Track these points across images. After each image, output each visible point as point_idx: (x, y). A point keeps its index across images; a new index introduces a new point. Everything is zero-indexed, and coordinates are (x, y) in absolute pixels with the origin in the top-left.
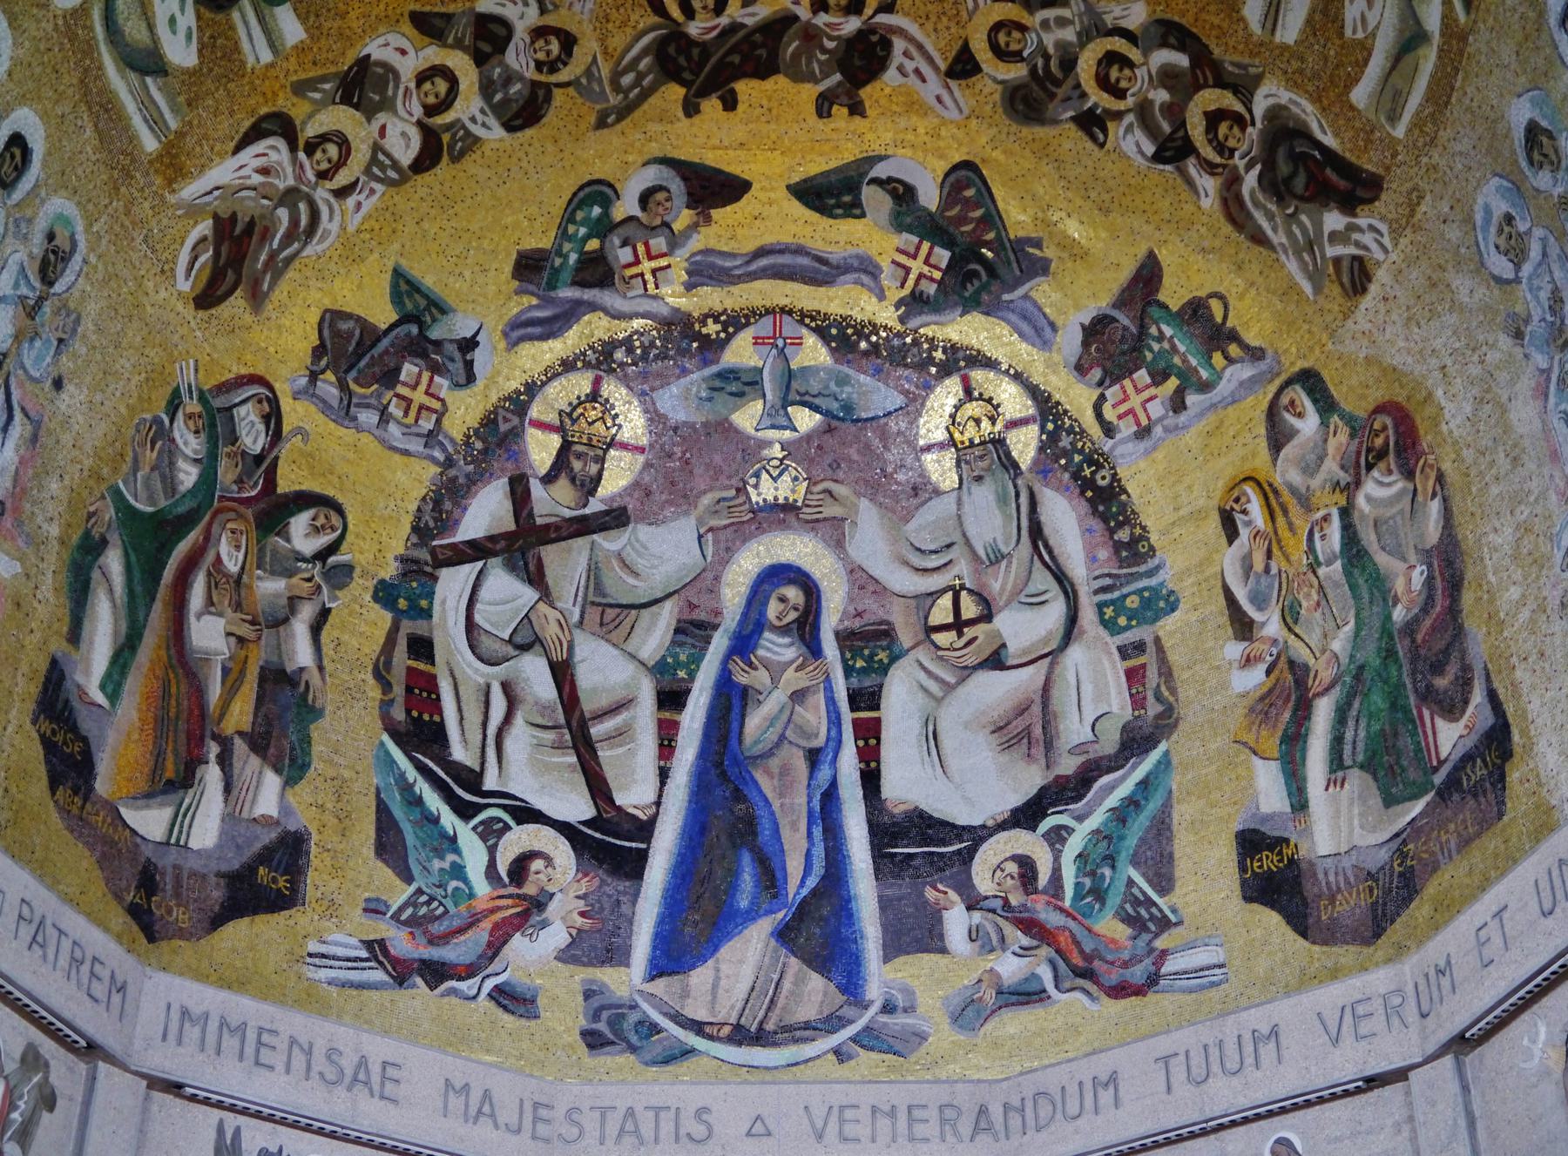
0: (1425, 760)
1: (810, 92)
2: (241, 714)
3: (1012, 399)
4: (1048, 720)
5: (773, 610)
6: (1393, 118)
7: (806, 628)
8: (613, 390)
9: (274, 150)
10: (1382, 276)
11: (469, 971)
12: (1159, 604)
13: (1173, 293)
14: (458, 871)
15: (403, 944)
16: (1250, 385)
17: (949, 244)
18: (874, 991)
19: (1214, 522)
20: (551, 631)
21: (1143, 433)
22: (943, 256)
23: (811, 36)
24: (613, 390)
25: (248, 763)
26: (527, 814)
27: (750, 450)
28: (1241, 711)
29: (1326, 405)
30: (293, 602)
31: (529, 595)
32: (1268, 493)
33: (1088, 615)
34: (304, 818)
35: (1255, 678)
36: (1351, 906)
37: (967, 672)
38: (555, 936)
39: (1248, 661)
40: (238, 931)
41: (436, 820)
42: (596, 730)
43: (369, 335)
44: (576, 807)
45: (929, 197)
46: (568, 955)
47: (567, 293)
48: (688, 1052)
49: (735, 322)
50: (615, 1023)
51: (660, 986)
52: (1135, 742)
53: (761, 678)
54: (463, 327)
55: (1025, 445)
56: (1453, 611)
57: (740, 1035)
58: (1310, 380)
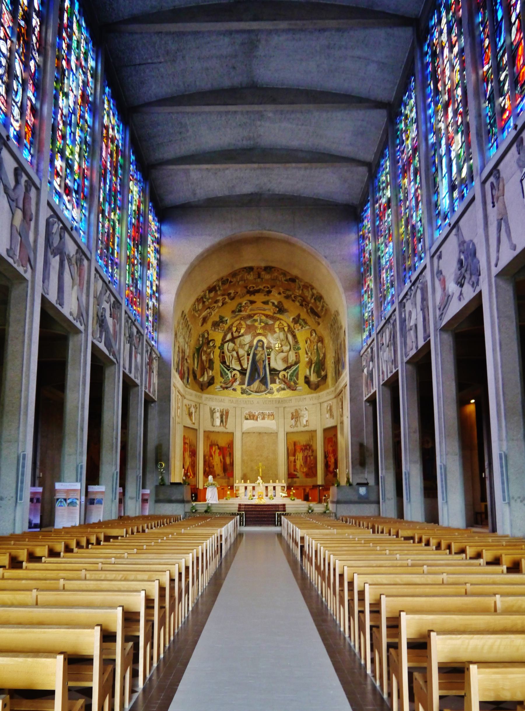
0: (321, 374)
1: (263, 294)
2: (207, 366)
3: (285, 325)
4: (287, 359)
5: (259, 344)
6: (322, 312)
7: (263, 347)
8: (243, 322)
9: (208, 310)
10: (321, 325)
11: (230, 387)
12: (299, 349)
13: (302, 317)
14: (228, 377)
15: (224, 386)
16: (309, 329)
17: (278, 308)
18: (269, 388)
19: (305, 342)
20: (236, 348)
21: (298, 330)
22: (278, 309)
23: (263, 290)
24: (243, 322)
25: (208, 370)
26: (234, 370)
27: (256, 328)
28: (306, 363)
29: (316, 334)
30: (211, 352)
31: (233, 345)
32: (310, 340)
33: (292, 348)
34: (214, 374)
35: (307, 359)
36: (313, 386)
37: (279, 353)
38: (238, 382)
39: (307, 357)
40: (210, 388)
41: (225, 372)
42: (241, 359)
43: (217, 322)
44: (239, 368)
45: (276, 303)
46: (240, 384)
47: (237, 313)
48: (251, 394)
49: (255, 314)
50: (244, 391)
51: (248, 387)
52: (296, 363)
53: (258, 352)
54: (226, 319)
55: (286, 329)
56: (324, 361)
57: (256, 392)
58: (314, 330)
